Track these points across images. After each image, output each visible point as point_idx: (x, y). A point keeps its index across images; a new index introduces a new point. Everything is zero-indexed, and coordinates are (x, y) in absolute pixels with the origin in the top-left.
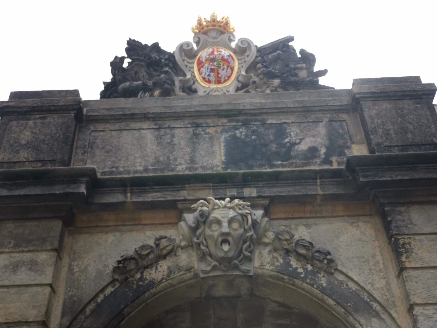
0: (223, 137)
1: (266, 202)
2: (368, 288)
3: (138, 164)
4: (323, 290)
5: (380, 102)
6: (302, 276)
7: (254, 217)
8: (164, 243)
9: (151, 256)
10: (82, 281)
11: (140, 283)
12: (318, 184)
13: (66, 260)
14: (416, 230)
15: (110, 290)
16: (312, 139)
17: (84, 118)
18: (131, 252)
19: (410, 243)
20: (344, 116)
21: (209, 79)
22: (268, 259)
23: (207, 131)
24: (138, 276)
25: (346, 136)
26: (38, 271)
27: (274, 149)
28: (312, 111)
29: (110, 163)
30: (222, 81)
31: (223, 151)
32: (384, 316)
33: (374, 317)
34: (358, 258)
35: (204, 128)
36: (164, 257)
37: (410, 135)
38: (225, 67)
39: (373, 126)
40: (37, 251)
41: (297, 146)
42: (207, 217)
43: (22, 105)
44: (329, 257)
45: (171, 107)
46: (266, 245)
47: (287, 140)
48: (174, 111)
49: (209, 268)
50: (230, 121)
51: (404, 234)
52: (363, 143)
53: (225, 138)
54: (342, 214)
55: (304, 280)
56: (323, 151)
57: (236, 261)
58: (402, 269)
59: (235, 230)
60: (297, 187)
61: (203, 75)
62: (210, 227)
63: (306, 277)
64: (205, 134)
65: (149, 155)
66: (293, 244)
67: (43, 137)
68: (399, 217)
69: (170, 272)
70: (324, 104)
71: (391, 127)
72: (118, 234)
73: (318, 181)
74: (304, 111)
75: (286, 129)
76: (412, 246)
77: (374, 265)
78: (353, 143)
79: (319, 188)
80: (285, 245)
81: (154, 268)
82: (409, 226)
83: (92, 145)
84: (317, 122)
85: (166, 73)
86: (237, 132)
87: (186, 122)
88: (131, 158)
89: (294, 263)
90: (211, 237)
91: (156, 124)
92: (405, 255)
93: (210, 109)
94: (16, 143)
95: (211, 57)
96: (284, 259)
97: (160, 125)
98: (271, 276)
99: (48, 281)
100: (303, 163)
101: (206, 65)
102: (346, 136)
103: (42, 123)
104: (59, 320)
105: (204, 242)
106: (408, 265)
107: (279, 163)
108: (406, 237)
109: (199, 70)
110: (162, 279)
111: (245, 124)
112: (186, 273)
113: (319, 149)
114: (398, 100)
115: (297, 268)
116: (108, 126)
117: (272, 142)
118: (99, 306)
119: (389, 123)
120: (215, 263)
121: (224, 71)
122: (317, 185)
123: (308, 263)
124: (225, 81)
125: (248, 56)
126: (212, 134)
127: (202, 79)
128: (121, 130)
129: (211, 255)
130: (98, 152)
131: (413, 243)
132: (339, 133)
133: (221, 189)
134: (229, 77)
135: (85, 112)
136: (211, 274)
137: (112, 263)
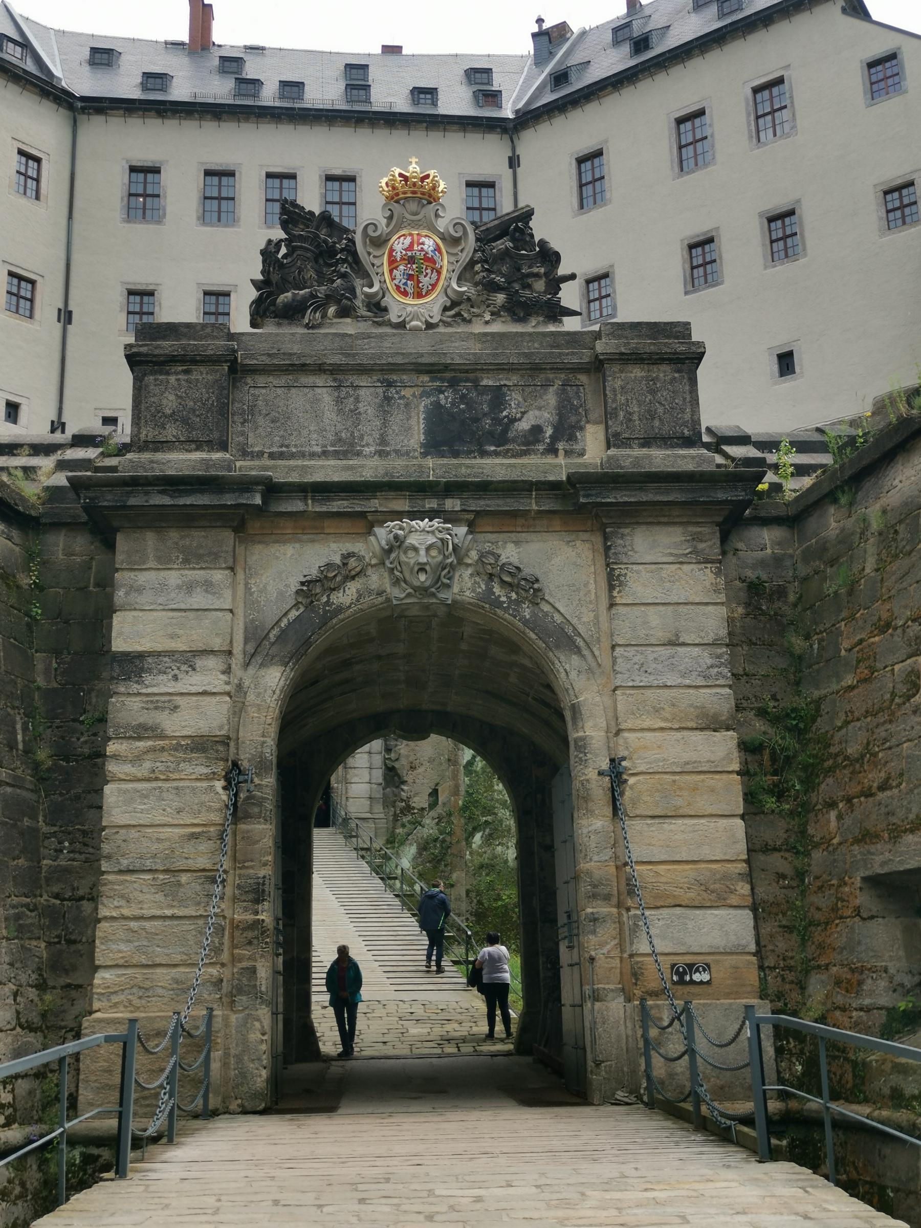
1: (471, 516)
2: (574, 621)
3: (313, 443)
4: (526, 622)
5: (630, 367)
7: (456, 541)
9: (338, 579)
10: (262, 603)
13: (240, 575)
14: (637, 558)
15: (294, 614)
16: (537, 413)
17: (239, 368)
18: (314, 573)
20: (583, 378)
22: (469, 585)
23: (403, 393)
24: (325, 599)
25: (580, 410)
26: (215, 593)
28: (541, 369)
29: (278, 438)
31: (422, 426)
33: (575, 654)
34: (569, 586)
35: (398, 389)
36: (353, 578)
37: (657, 423)
38: (429, 271)
39: (614, 406)
40: (210, 568)
41: (516, 424)
42: (402, 542)
43: (157, 352)
44: (536, 586)
45: (354, 355)
46: (468, 565)
47: (505, 413)
48: (359, 362)
49: (402, 596)
50: (433, 380)
51: (621, 563)
52: (601, 423)
53: (426, 406)
54: (558, 529)
55: (506, 610)
56: (549, 432)
57: (433, 590)
58: (612, 605)
59: (434, 557)
60: (508, 500)
61: (396, 282)
62: (405, 553)
63: (508, 607)
64: (400, 398)
65: (328, 428)
67: (192, 403)
68: (620, 542)
69: (360, 595)
70: (558, 360)
71: (636, 409)
72: (297, 545)
73: (534, 493)
74: (530, 369)
75: (504, 395)
76: (628, 578)
77: (585, 595)
78: (588, 422)
79: (533, 501)
80: (489, 569)
81: (342, 591)
82: (630, 553)
83: (252, 409)
85: (344, 276)
86: (442, 396)
87: (375, 378)
88: (305, 432)
89: (497, 590)
90: (408, 564)
91: (335, 380)
92: (617, 589)
93: (407, 361)
94: (159, 412)
95: (409, 254)
96: (487, 585)
97: (340, 381)
98: (470, 603)
100: (521, 450)
101: (402, 268)
102: (580, 410)
103: (187, 381)
104: (242, 646)
105: (399, 568)
106: (618, 601)
107: (493, 448)
108: (623, 566)
109: (391, 271)
110: (351, 604)
111: (453, 383)
113: (545, 428)
114: (653, 364)
115: (500, 596)
116: (271, 379)
117: (485, 415)
118: (283, 632)
119: (635, 402)
120: (410, 590)
121: (427, 278)
122: (531, 498)
123: (512, 591)
124: (427, 294)
125: (462, 251)
128: (289, 387)
129: (405, 581)
130: (261, 421)
131: (629, 574)
132: (573, 404)
134: (434, 286)
135: (239, 361)
136: (404, 601)
137: (294, 586)
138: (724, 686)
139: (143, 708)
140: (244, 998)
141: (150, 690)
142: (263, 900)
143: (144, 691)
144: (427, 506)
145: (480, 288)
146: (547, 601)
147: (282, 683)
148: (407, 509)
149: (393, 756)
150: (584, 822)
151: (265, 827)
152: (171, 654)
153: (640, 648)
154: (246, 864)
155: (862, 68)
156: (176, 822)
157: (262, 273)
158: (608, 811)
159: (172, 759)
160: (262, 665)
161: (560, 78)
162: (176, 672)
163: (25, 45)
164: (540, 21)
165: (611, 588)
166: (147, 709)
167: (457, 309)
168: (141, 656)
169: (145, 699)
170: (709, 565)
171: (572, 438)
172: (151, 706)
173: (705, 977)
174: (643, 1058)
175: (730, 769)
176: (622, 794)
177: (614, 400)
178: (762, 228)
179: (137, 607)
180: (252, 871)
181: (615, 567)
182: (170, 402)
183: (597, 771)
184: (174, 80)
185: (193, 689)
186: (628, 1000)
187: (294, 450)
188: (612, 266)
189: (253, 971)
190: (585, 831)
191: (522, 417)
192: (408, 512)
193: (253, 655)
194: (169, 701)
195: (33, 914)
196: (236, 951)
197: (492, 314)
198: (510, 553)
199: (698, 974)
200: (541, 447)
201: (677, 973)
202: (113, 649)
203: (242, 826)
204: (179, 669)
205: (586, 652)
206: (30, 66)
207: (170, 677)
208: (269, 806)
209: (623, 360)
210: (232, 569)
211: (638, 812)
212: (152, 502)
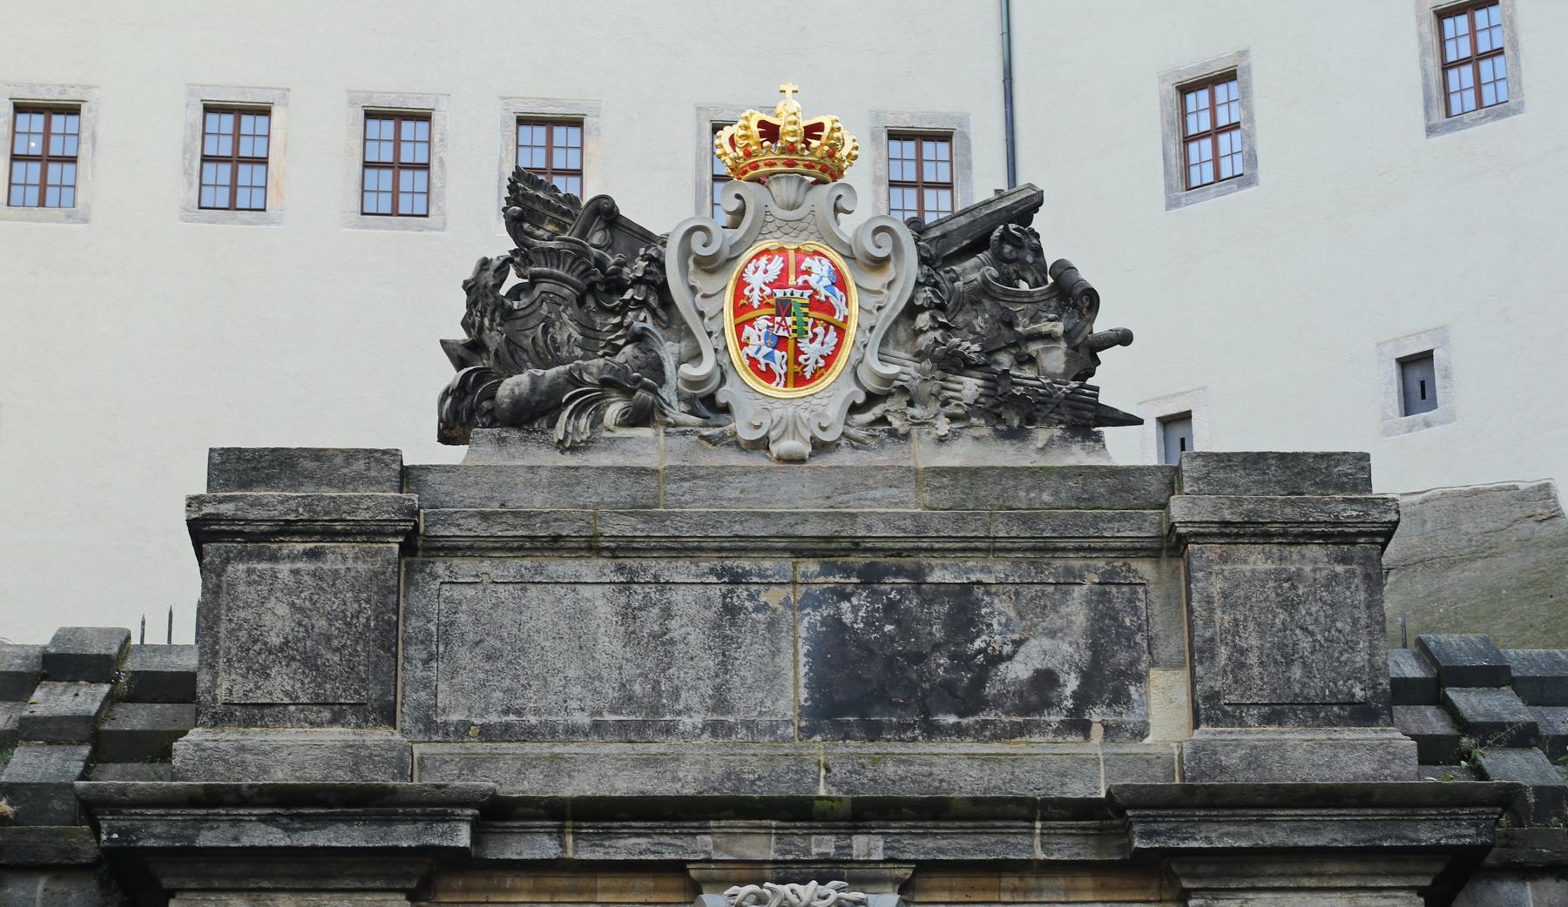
1: (905, 872)
3: (574, 704)
5: (1242, 550)
12: (1038, 831)
16: (1047, 643)
17: (420, 543)
20: (1144, 568)
21: (767, 365)
23: (763, 598)
25: (1138, 638)
27: (941, 671)
28: (1056, 550)
29: (499, 694)
30: (808, 375)
31: (803, 670)
35: (753, 588)
37: (1297, 672)
38: (820, 330)
39: (1208, 634)
41: (1002, 667)
43: (253, 514)
45: (663, 518)
47: (978, 644)
48: (672, 532)
50: (827, 570)
52: (1180, 665)
53: (811, 627)
56: (1072, 684)
60: (984, 839)
61: (750, 350)
64: (757, 609)
65: (604, 673)
67: (323, 623)
70: (1091, 532)
71: (1254, 642)
74: (1033, 549)
75: (978, 603)
78: (1153, 664)
79: (1037, 841)
83: (446, 631)
84: (1070, 579)
85: (639, 338)
86: (845, 606)
87: (705, 566)
88: (556, 682)
91: (620, 569)
93: (772, 531)
94: (255, 642)
95: (779, 293)
97: (631, 571)
100: (1013, 724)
101: (762, 323)
102: (1138, 638)
103: (314, 574)
107: (952, 719)
109: (739, 328)
111: (870, 577)
113: (1062, 678)
114: (1290, 544)
116: (486, 565)
117: (936, 647)
119: (1251, 625)
121: (817, 344)
122: (1032, 835)
124: (813, 378)
125: (890, 285)
126: (774, 611)
127: (747, 362)
128: (523, 584)
130: (463, 656)
132: (1121, 625)
133: (796, 834)
134: (829, 359)
135: (422, 530)
144: (815, 850)
145: (927, 365)
148: (772, 855)
157: (466, 324)
167: (877, 411)
171: (1120, 698)
177: (1209, 622)
182: (278, 621)
187: (533, 720)
188: (1243, 54)
191: (1015, 652)
192: (775, 862)
200: (1054, 718)
209: (1228, 535)
212: (246, 841)
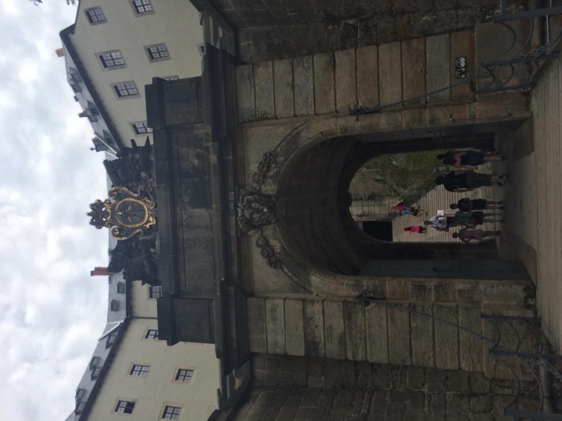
0: (189, 209)
2: (284, 136)
6: (278, 169)
8: (260, 243)
9: (268, 249)
10: (281, 284)
11: (282, 254)
13: (269, 295)
14: (253, 106)
15: (286, 270)
18: (265, 260)
19: (261, 112)
24: (278, 255)
32: (299, 130)
35: (183, 221)
36: (268, 242)
40: (265, 309)
44: (268, 155)
46: (260, 188)
47: (191, 171)
51: (256, 114)
56: (199, 150)
57: (271, 205)
58: (276, 118)
62: (254, 219)
64: (187, 220)
66: (261, 173)
68: (246, 115)
76: (262, 110)
80: (261, 178)
81: (274, 247)
82: (251, 110)
86: (185, 201)
89: (271, 173)
92: (268, 115)
99: (282, 301)
106: (273, 115)
107: (207, 177)
108: (257, 113)
110: (280, 243)
112: (277, 230)
115: (274, 172)
118: (294, 275)
120: (272, 215)
123: (271, 166)
126: (187, 216)
129: (268, 218)
131: (261, 110)
135: (173, 293)
137: (272, 270)
138: (313, 60)
139: (331, 342)
140: (475, 296)
141: (323, 339)
142: (424, 286)
143: (323, 341)
144: (232, 208)
145: (139, 184)
146: (276, 149)
147: (318, 276)
148: (234, 218)
149: (363, 197)
150: (382, 127)
151: (387, 285)
152: (305, 328)
153: (296, 103)
154: (406, 294)
155: (93, 25)
156: (386, 328)
157: (139, 280)
158: (376, 115)
159: (355, 329)
160: (310, 284)
161: (109, 142)
162: (313, 326)
163: (110, 335)
164: (92, 149)
165: (267, 118)
166: (331, 340)
167: (149, 194)
168: (306, 342)
169: (327, 341)
170: (255, 70)
172: (330, 339)
173: (463, 60)
174: (507, 91)
175: (354, 54)
176: (367, 108)
178: (155, 61)
179: (284, 343)
180: (410, 291)
181: (257, 117)
183: (356, 122)
184: (120, 281)
185: (322, 318)
186: (475, 100)
187: (212, 269)
189: (460, 291)
190: (386, 126)
191: (193, 163)
192: (235, 217)
193: (305, 289)
194: (327, 330)
195: (433, 397)
196: (450, 300)
197: (150, 178)
198: (254, 168)
199: (461, 64)
201: (460, 75)
202: (304, 355)
203: (387, 295)
204: (312, 325)
205: (299, 130)
206: (116, 334)
207: (316, 329)
208: (377, 282)
210: (265, 299)
211: (377, 100)
212: (235, 337)
